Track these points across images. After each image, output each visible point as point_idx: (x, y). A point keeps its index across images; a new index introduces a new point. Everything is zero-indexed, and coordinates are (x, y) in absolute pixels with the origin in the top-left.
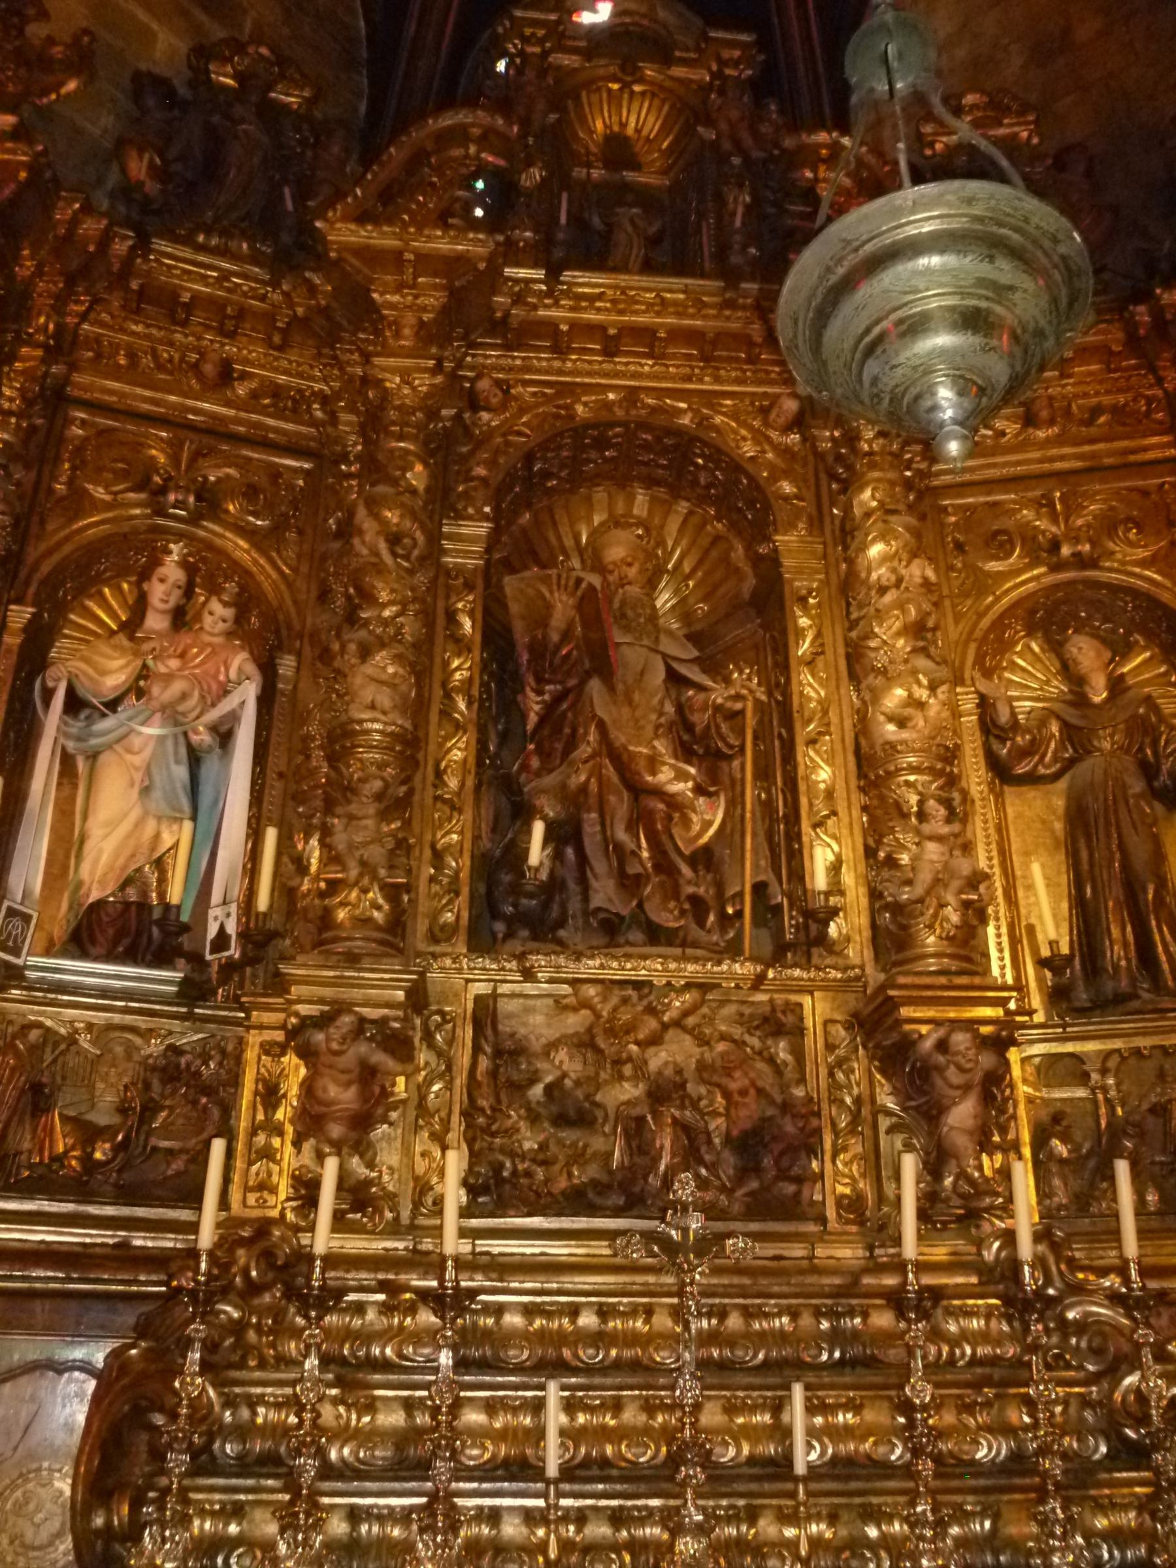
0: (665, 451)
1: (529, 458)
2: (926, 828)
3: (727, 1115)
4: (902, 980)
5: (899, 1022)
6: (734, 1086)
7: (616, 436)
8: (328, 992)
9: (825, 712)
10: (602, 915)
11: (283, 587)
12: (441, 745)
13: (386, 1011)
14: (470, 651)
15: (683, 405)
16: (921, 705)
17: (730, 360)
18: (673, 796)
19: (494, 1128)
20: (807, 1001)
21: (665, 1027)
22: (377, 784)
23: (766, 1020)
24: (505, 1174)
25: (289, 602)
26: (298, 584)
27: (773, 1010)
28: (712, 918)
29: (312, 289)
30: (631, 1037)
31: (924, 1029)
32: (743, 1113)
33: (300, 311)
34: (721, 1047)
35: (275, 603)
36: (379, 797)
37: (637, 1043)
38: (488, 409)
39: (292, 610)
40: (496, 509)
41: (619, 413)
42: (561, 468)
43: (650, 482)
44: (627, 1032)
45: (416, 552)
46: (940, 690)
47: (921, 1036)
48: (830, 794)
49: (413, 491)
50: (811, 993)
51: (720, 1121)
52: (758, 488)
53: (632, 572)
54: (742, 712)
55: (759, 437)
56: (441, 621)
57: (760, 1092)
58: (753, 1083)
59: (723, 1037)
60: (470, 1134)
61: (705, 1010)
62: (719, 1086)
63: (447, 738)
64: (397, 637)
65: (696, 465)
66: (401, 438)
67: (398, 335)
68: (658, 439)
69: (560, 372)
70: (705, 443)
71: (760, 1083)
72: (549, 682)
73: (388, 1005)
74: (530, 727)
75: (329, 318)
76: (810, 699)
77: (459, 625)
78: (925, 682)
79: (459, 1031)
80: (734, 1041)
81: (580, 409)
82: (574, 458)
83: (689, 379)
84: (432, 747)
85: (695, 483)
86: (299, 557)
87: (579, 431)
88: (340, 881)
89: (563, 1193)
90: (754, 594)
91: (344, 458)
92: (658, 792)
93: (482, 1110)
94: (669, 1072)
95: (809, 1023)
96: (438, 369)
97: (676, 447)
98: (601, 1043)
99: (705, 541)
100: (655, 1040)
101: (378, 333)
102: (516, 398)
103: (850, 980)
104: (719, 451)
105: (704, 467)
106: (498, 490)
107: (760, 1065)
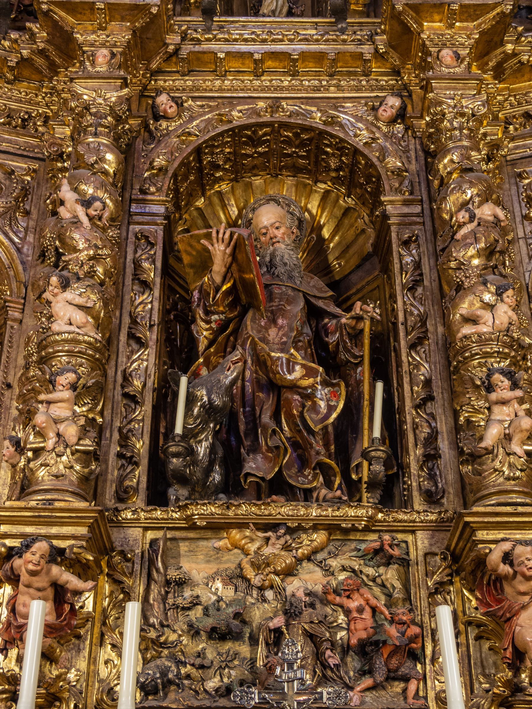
0: (302, 145)
1: (198, 151)
2: (493, 396)
3: (348, 630)
4: (475, 509)
5: (476, 543)
6: (353, 604)
7: (265, 134)
8: (29, 530)
9: (424, 323)
10: (250, 479)
11: (13, 251)
12: (129, 358)
13: (73, 542)
14: (151, 290)
15: (314, 109)
16: (490, 307)
17: (349, 74)
18: (305, 388)
19: (162, 639)
20: (410, 538)
21: (299, 561)
22: (71, 377)
23: (376, 552)
24: (170, 676)
25: (18, 262)
26: (25, 250)
27: (382, 545)
28: (338, 481)
29: (33, 35)
30: (271, 569)
31: (493, 546)
32: (360, 625)
33: (25, 52)
34: (342, 576)
35: (6, 262)
36: (73, 387)
37: (277, 573)
38: (166, 117)
39: (20, 268)
40: (176, 191)
41: (267, 118)
42: (225, 163)
43: (296, 170)
44: (268, 565)
45: (106, 215)
46: (505, 296)
47: (491, 550)
48: (428, 383)
49: (105, 173)
50: (413, 532)
51: (344, 633)
52: (373, 165)
53: (279, 233)
54: (362, 331)
55: (371, 126)
56: (130, 270)
57: (374, 610)
58: (367, 601)
59: (344, 569)
60: (142, 647)
61: (331, 548)
62: (342, 607)
63: (132, 352)
64: (91, 274)
65: (327, 153)
66: (96, 135)
67: (93, 64)
68: (297, 135)
69: (220, 90)
70: (332, 136)
71: (373, 602)
72: (214, 313)
73: (74, 537)
74: (201, 347)
75: (47, 58)
76: (412, 314)
77: (144, 271)
78: (493, 289)
79: (137, 567)
80: (354, 571)
81: (235, 113)
82: (234, 153)
83: (317, 89)
84: (123, 359)
85: (328, 169)
86: (26, 230)
87: (236, 132)
88: (43, 448)
89: (217, 690)
90: (375, 246)
91: (60, 156)
92: (293, 387)
93: (153, 626)
94: (300, 594)
95: (413, 556)
96: (125, 84)
97: (310, 140)
98: (250, 573)
99: (338, 213)
100: (289, 572)
101: (82, 63)
102: (189, 109)
103: (442, 521)
104: (342, 140)
105: (333, 155)
106: (175, 176)
107: (377, 590)
